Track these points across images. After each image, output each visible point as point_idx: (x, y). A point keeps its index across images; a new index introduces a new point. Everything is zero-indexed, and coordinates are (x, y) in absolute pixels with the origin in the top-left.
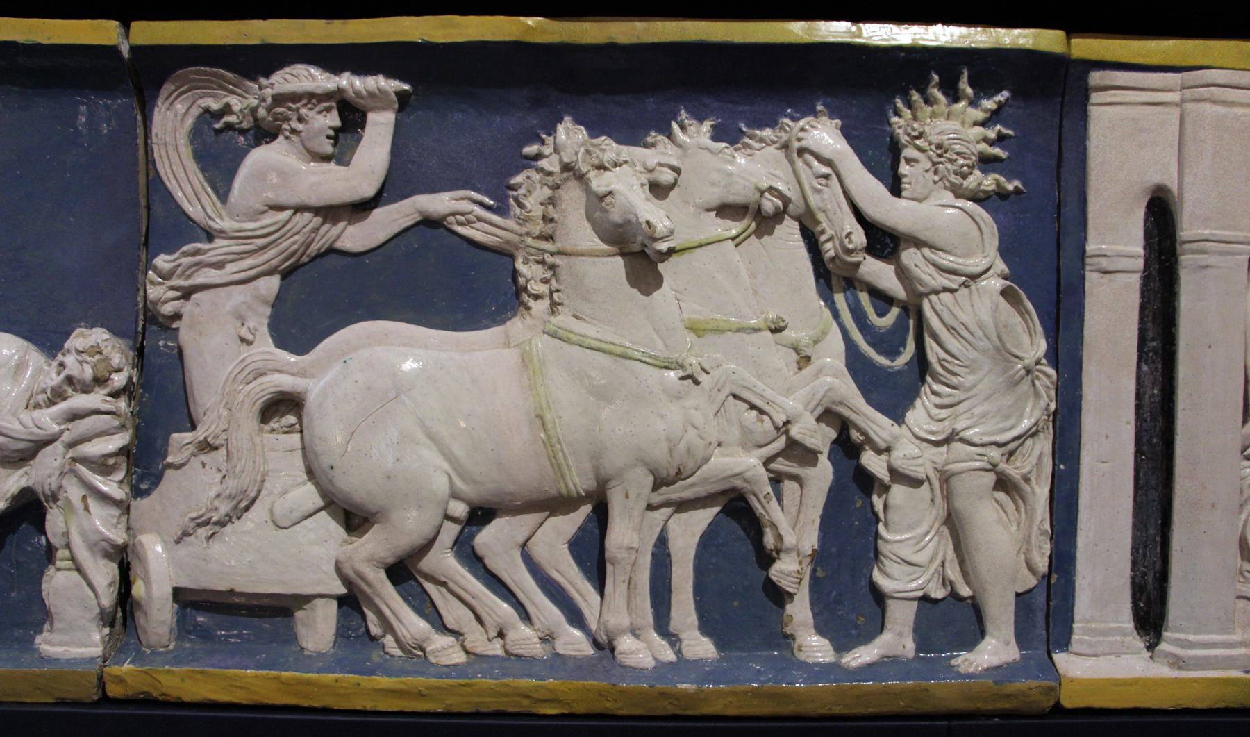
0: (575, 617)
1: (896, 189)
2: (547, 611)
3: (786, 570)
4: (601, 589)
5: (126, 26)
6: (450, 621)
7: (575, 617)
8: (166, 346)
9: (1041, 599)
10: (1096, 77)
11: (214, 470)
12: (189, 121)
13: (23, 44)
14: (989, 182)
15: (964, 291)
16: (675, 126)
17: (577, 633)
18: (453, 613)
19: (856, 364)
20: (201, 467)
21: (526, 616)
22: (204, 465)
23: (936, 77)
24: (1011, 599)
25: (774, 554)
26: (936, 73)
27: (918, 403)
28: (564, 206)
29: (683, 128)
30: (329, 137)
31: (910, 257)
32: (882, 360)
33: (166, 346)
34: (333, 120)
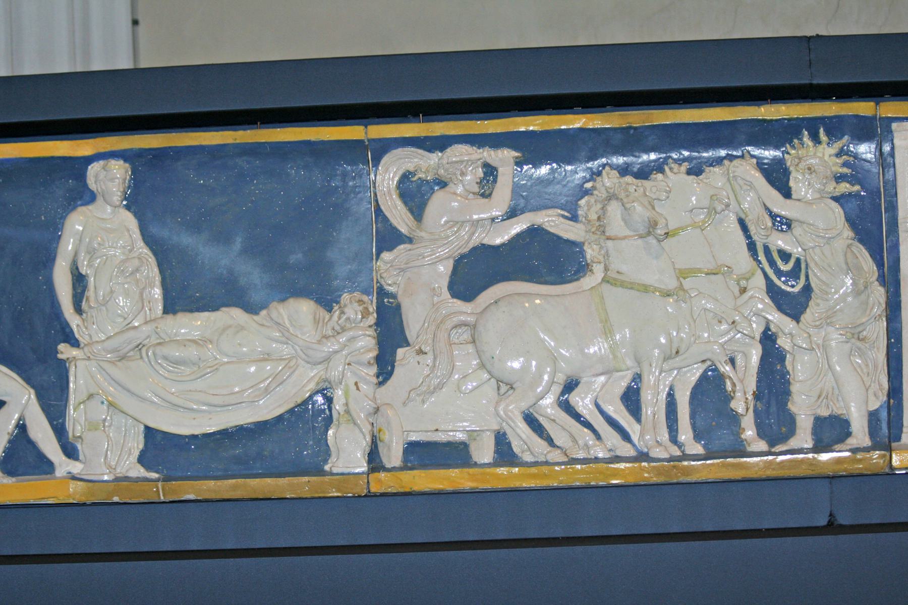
0: (626, 436)
1: (787, 193)
2: (611, 437)
3: (738, 405)
4: (639, 420)
5: (366, 127)
6: (558, 442)
7: (626, 436)
8: (388, 302)
9: (884, 415)
10: (894, 126)
11: (425, 365)
12: (397, 179)
13: (314, 141)
14: (845, 187)
15: (827, 246)
16: (666, 168)
17: (629, 445)
18: (560, 439)
19: (773, 291)
20: (417, 364)
21: (598, 437)
22: (419, 363)
23: (806, 133)
24: (866, 415)
25: (732, 394)
26: (806, 130)
27: (808, 310)
28: (609, 214)
29: (671, 169)
30: (477, 183)
31: (797, 230)
32: (789, 289)
33: (388, 302)
34: (480, 172)
